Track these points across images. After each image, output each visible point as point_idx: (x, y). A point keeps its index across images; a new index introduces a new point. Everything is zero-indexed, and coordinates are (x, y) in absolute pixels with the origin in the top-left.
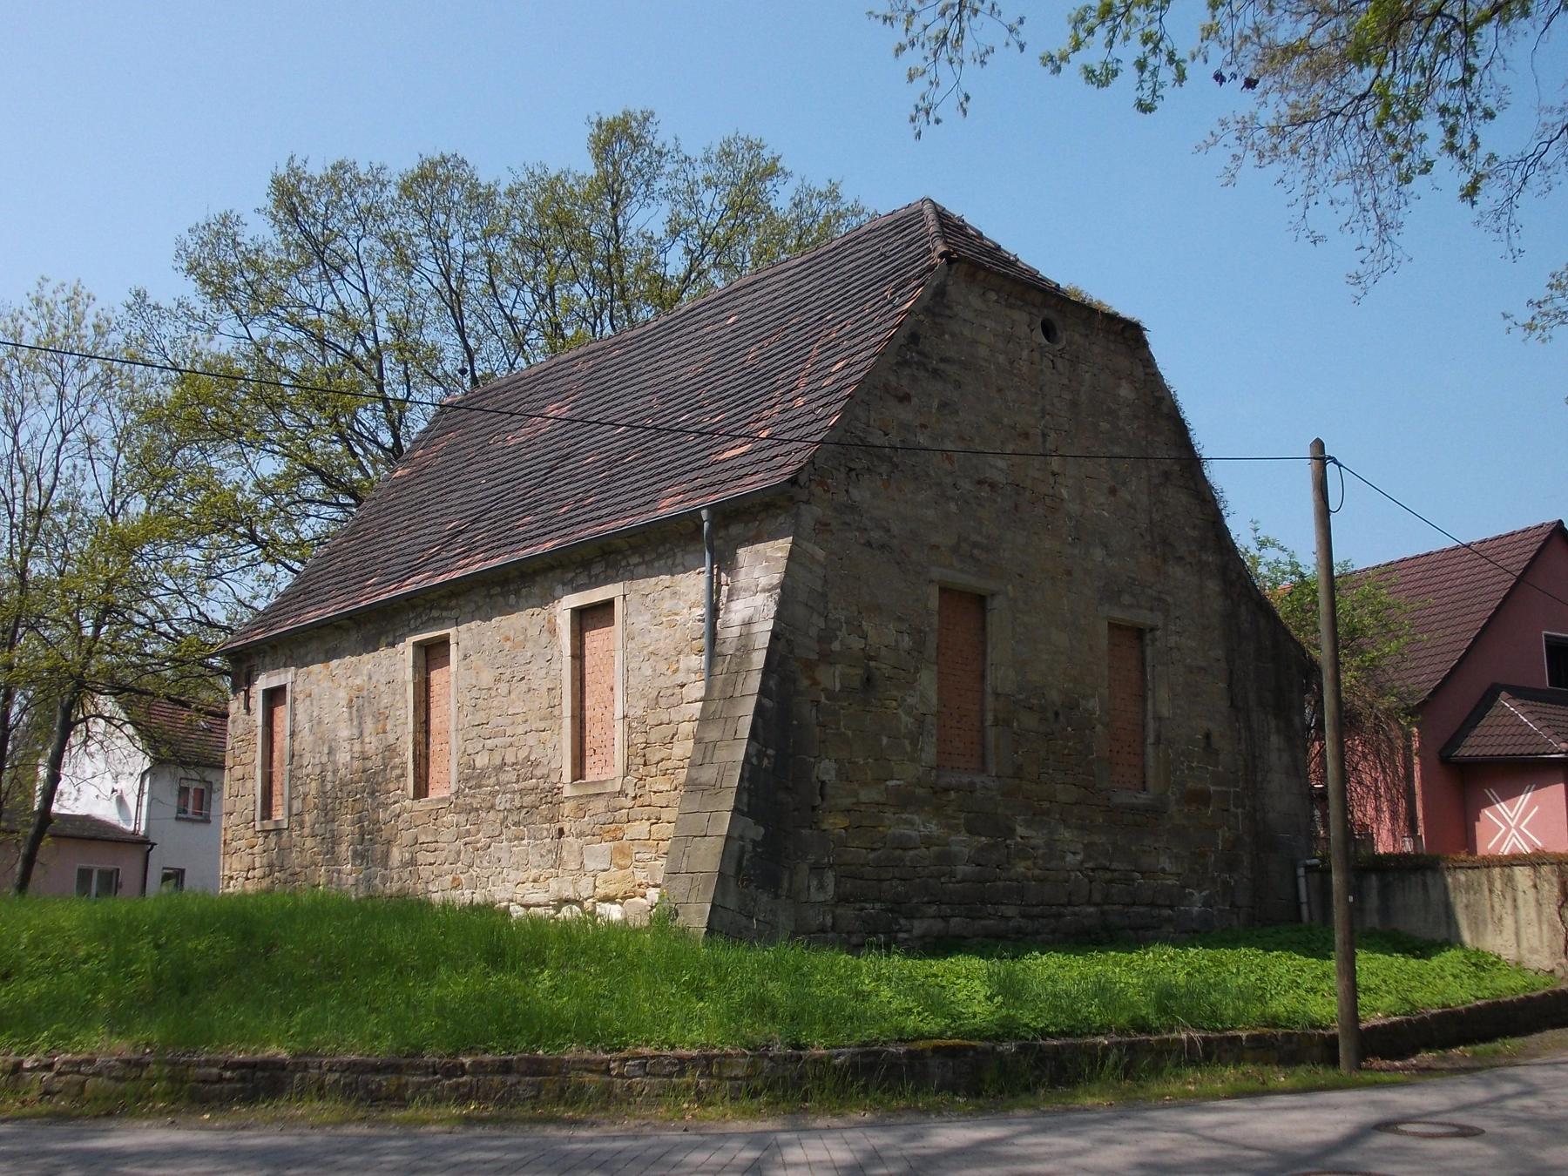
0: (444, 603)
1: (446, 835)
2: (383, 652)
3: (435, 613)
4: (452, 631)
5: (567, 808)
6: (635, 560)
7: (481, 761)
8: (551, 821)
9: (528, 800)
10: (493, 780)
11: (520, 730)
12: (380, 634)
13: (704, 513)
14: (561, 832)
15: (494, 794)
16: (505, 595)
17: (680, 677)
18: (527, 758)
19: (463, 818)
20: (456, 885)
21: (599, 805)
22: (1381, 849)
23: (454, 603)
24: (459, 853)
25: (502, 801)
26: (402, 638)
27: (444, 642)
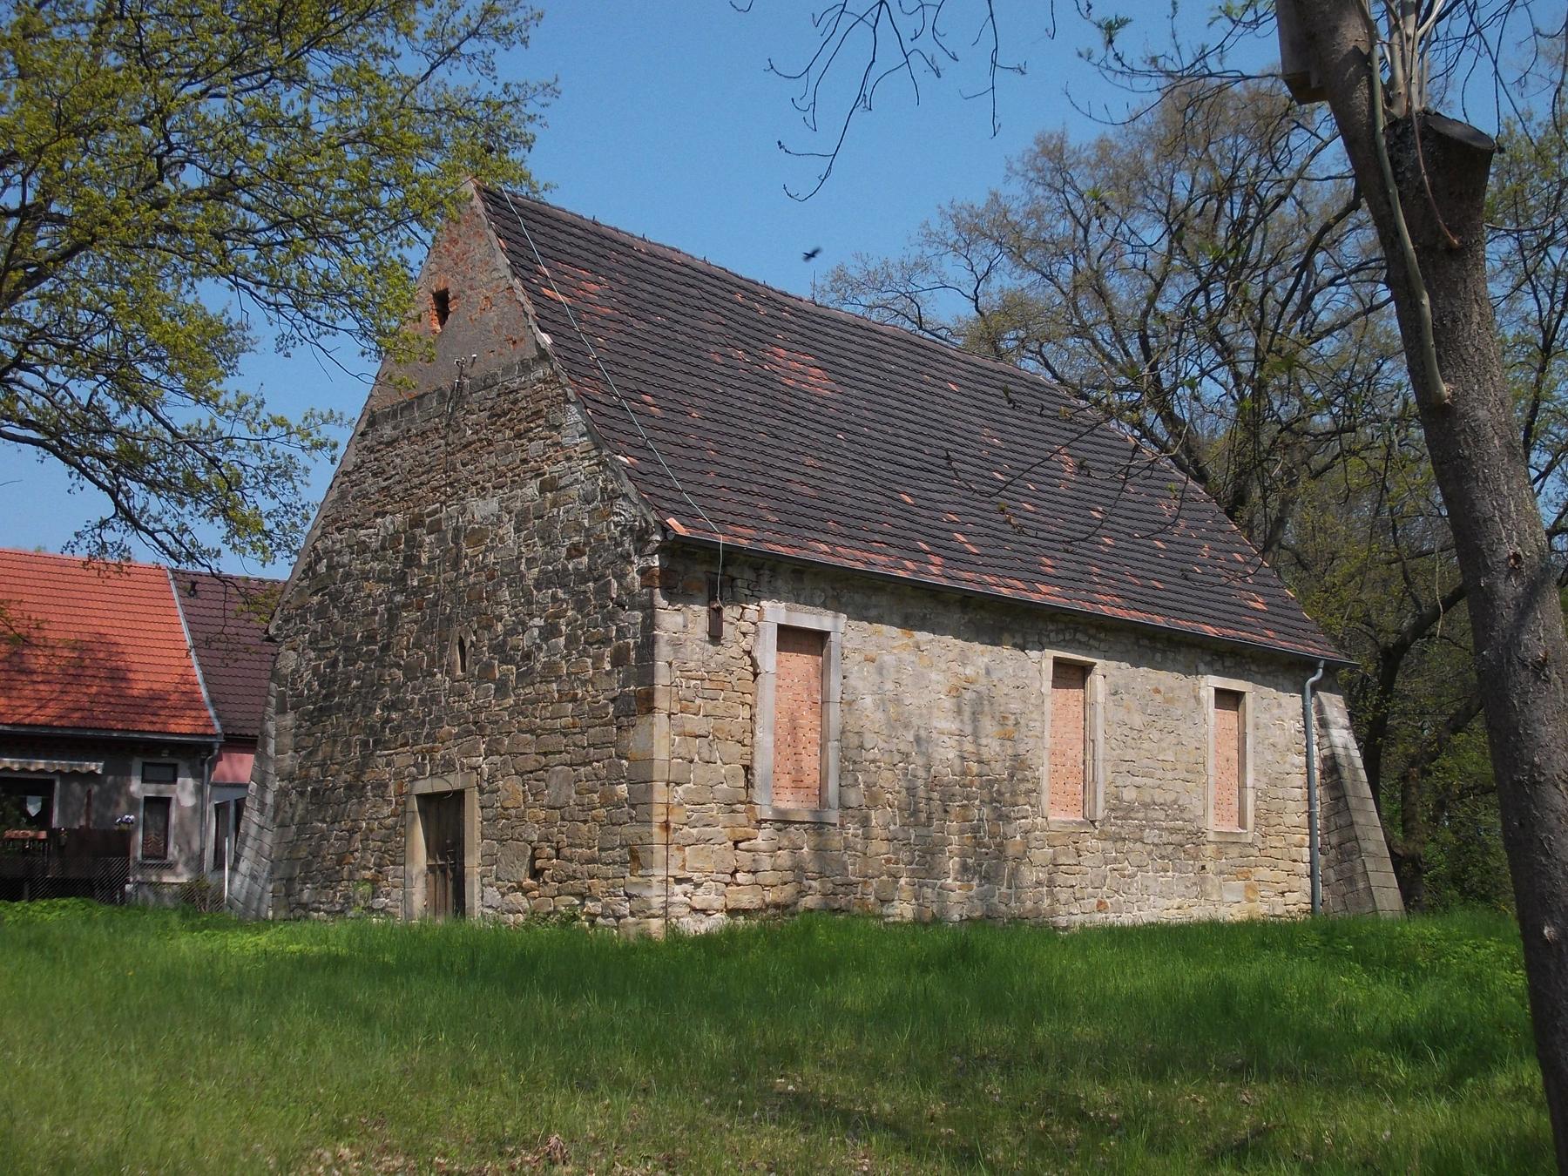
0: (1092, 631)
1: (1088, 860)
2: (1006, 651)
3: (1079, 636)
4: (1100, 663)
5: (1209, 850)
6: (1254, 668)
7: (1129, 795)
8: (1195, 859)
9: (1176, 838)
10: (1141, 815)
11: (1169, 775)
12: (1002, 630)
13: (1322, 664)
14: (1203, 868)
15: (1142, 828)
16: (1154, 650)
17: (1287, 768)
18: (1175, 802)
19: (1109, 845)
20: (1101, 906)
21: (1234, 852)
22: (1535, 1121)
23: (1102, 636)
24: (1105, 878)
25: (1150, 835)
26: (1053, 645)
27: (1085, 670)
